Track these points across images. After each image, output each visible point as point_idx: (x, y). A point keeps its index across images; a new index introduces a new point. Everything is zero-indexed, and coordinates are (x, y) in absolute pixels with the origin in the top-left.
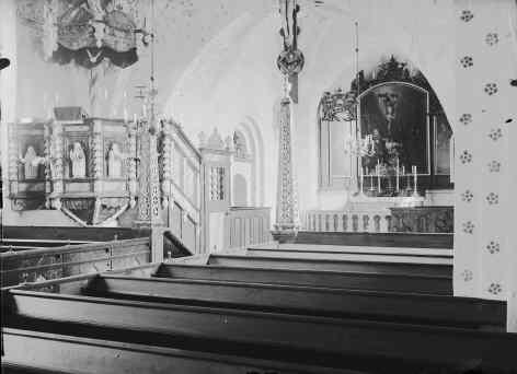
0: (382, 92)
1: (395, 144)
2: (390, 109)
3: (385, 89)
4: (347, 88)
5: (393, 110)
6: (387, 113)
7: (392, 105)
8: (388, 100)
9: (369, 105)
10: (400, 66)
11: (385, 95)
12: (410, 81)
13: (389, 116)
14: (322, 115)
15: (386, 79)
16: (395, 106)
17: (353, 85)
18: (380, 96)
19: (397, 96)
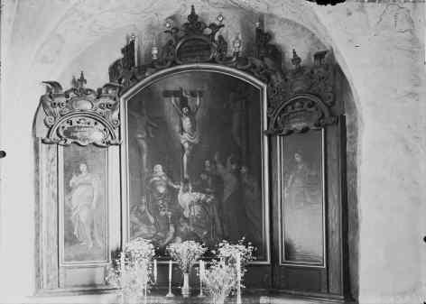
0: (171, 87)
1: (197, 195)
2: (187, 122)
3: (178, 79)
4: (98, 77)
5: (193, 122)
6: (182, 130)
7: (191, 114)
8: (184, 103)
9: (145, 109)
10: (208, 31)
11: (177, 93)
12: (225, 60)
13: (186, 136)
14: (42, 132)
15: (182, 56)
16: (198, 116)
17: (114, 70)
18: (167, 94)
19: (201, 94)
